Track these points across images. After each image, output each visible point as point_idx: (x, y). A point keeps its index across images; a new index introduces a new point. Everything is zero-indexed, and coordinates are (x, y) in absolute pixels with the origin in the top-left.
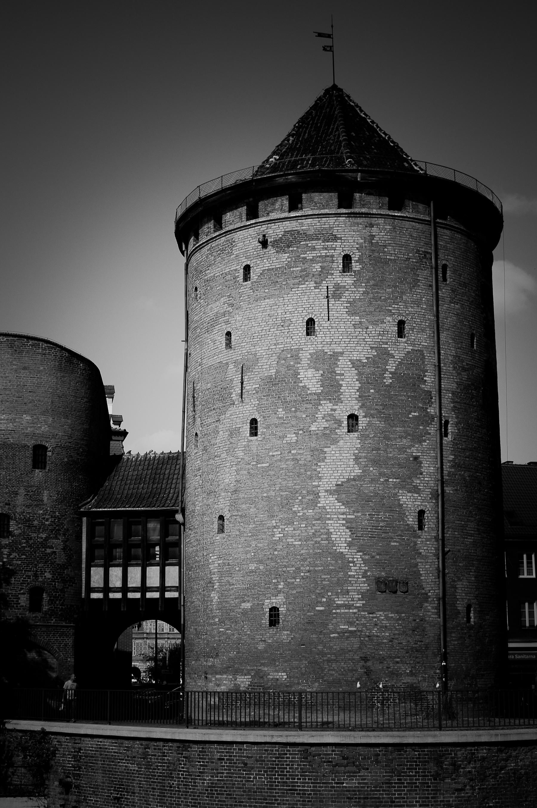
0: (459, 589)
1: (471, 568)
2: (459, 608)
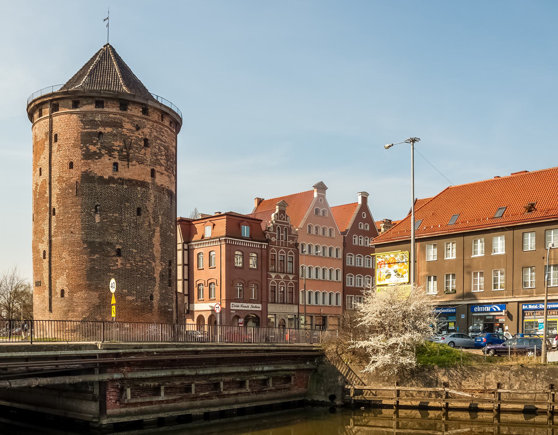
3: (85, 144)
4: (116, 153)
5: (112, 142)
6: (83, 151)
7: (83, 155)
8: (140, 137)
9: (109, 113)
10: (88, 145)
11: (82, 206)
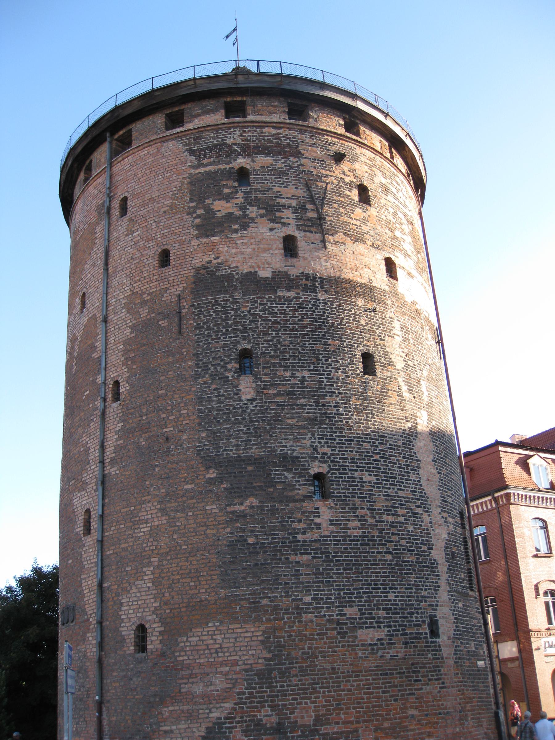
0: (125, 604)
1: (144, 569)
2: (123, 633)
3: (201, 201)
4: (288, 213)
5: (276, 189)
6: (198, 217)
7: (198, 227)
8: (347, 180)
9: (263, 125)
10: (208, 202)
11: (198, 360)
